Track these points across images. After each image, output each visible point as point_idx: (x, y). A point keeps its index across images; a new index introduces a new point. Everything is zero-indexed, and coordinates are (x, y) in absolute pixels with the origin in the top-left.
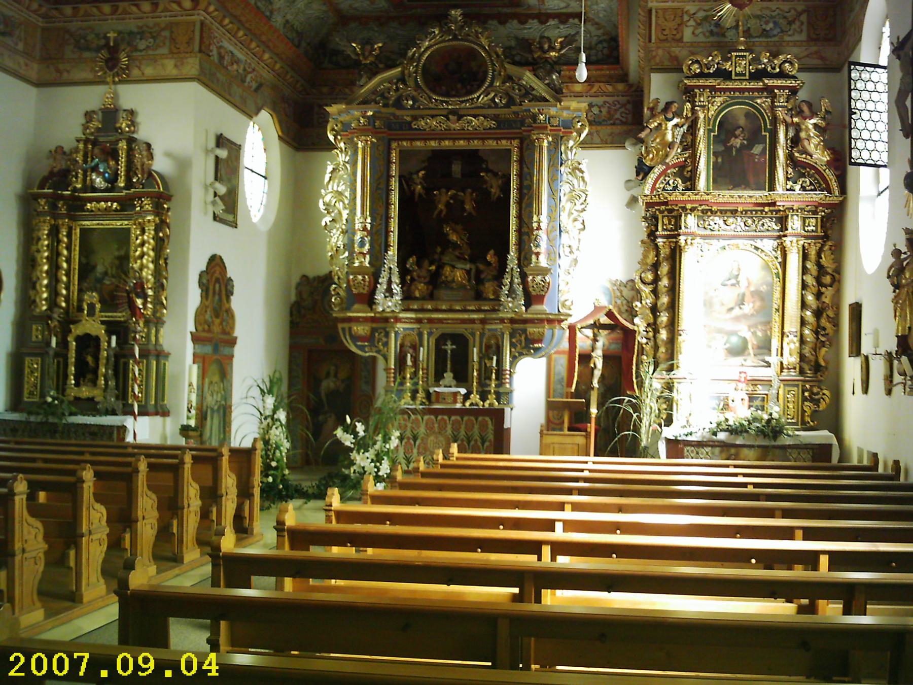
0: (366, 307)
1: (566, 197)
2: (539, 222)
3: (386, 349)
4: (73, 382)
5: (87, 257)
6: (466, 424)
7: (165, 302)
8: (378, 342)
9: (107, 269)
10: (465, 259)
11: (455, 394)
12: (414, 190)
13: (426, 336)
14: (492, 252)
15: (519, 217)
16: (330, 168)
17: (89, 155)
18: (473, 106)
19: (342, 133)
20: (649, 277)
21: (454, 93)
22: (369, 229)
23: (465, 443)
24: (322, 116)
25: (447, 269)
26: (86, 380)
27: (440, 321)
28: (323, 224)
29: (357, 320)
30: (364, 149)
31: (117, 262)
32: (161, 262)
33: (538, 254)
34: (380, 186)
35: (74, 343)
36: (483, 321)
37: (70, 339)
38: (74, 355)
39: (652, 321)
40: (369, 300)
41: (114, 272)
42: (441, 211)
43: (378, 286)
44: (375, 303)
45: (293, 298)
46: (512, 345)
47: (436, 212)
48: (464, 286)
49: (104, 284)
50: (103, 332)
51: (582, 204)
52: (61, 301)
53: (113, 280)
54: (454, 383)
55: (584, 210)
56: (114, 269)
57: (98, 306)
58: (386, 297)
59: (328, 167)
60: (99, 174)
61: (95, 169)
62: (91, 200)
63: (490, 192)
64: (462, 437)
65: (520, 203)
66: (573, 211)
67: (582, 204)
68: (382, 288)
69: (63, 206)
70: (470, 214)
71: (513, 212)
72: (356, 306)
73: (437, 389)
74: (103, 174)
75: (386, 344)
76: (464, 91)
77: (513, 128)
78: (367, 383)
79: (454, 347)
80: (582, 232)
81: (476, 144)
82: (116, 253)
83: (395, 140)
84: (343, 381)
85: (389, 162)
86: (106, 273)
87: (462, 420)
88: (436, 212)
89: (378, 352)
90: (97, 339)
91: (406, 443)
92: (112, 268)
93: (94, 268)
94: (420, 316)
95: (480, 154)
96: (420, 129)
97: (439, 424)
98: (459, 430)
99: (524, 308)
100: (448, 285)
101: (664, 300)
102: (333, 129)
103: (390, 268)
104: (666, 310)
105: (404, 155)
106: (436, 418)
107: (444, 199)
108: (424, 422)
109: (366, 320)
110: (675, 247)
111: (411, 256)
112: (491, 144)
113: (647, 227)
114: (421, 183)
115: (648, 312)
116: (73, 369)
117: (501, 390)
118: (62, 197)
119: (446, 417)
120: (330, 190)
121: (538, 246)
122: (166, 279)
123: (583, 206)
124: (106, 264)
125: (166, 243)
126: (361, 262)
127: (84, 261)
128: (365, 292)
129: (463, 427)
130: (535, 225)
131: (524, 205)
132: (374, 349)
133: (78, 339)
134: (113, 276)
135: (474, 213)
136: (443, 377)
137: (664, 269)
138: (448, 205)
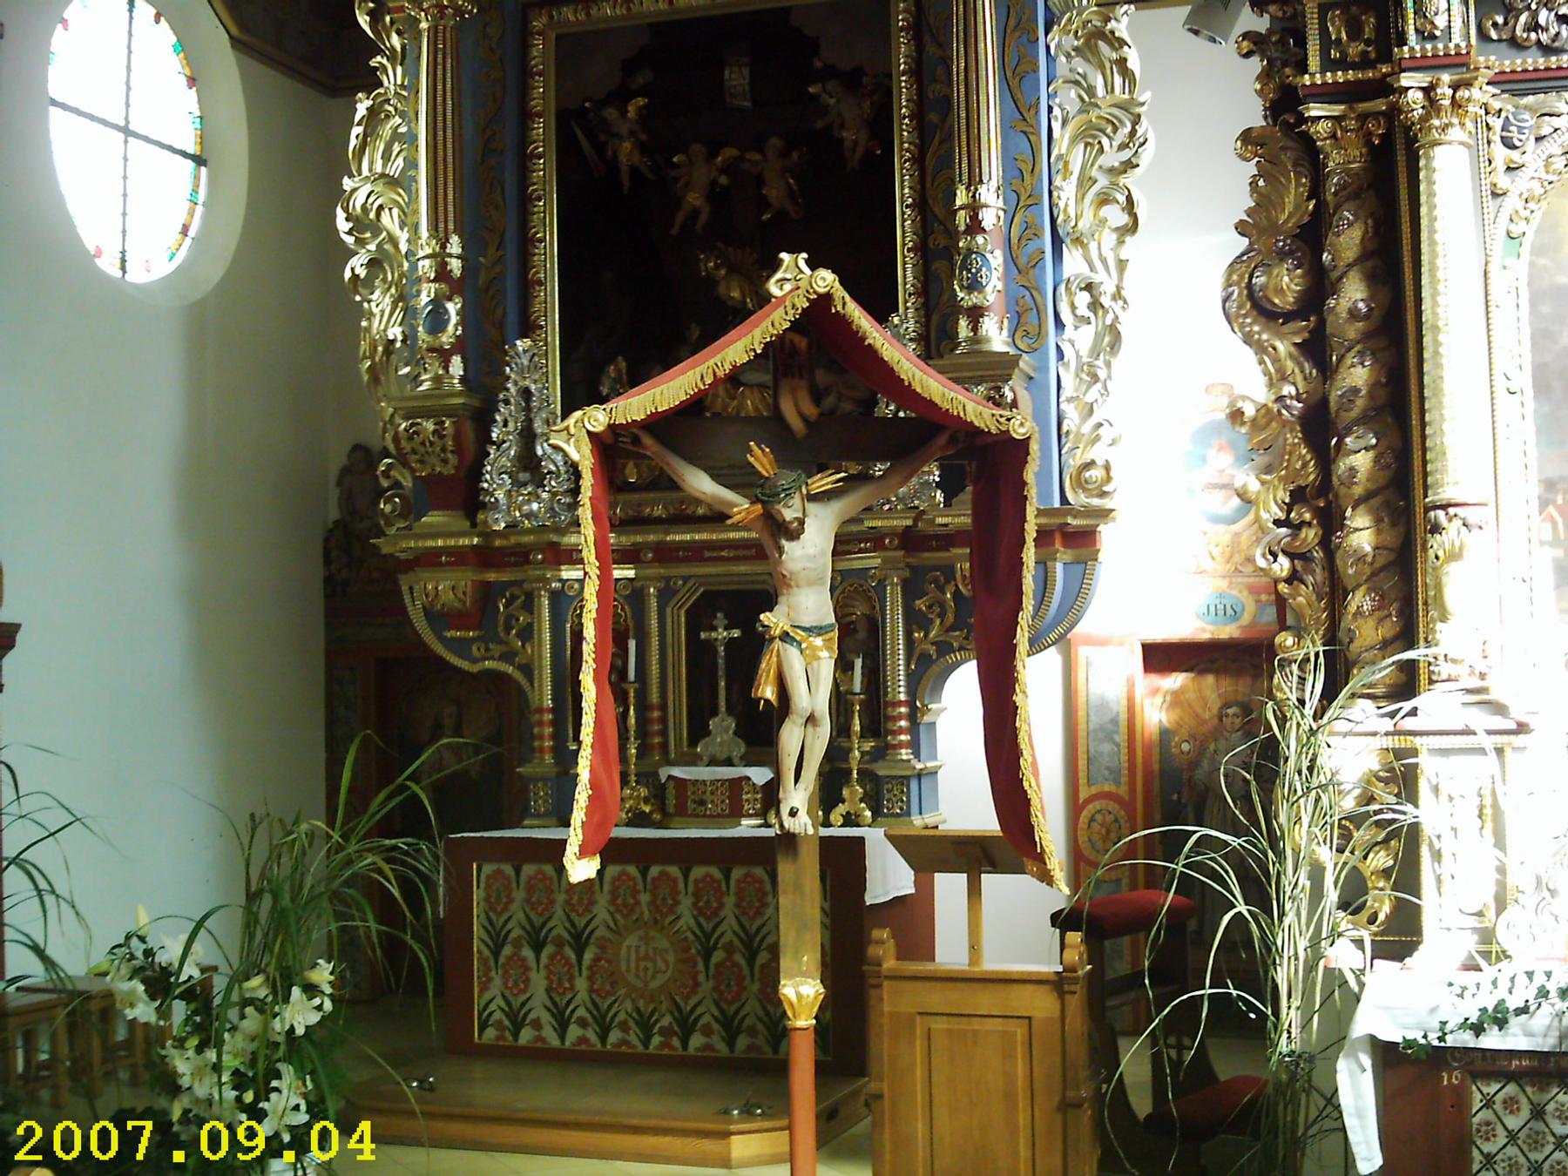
1: (1071, 127)
2: (974, 208)
6: (740, 891)
8: (508, 629)
11: (737, 785)
12: (615, 157)
15: (921, 205)
16: (362, 109)
20: (1287, 283)
22: (457, 272)
23: (739, 958)
28: (348, 274)
29: (429, 559)
33: (976, 314)
39: (1311, 475)
40: (471, 501)
42: (696, 212)
44: (484, 506)
45: (334, 513)
46: (914, 620)
47: (680, 218)
51: (1123, 146)
54: (740, 749)
55: (1130, 165)
63: (841, 141)
64: (728, 936)
65: (919, 160)
66: (1094, 173)
67: (1123, 146)
71: (903, 191)
72: (433, 519)
73: (677, 772)
75: (527, 633)
79: (736, 633)
80: (1128, 239)
87: (727, 878)
88: (680, 218)
89: (508, 657)
91: (552, 957)
97: (654, 895)
98: (716, 913)
99: (939, 496)
101: (1357, 375)
103: (526, 394)
104: (1363, 420)
105: (570, 48)
106: (644, 873)
107: (701, 175)
109: (459, 558)
110: (1387, 138)
111: (611, 359)
113: (1264, 76)
114: (632, 133)
115: (1294, 438)
117: (882, 770)
119: (674, 870)
120: (365, 172)
121: (974, 286)
123: (1127, 154)
126: (437, 380)
128: (449, 470)
129: (730, 900)
130: (962, 219)
131: (930, 163)
137: (1348, 240)
138: (715, 195)
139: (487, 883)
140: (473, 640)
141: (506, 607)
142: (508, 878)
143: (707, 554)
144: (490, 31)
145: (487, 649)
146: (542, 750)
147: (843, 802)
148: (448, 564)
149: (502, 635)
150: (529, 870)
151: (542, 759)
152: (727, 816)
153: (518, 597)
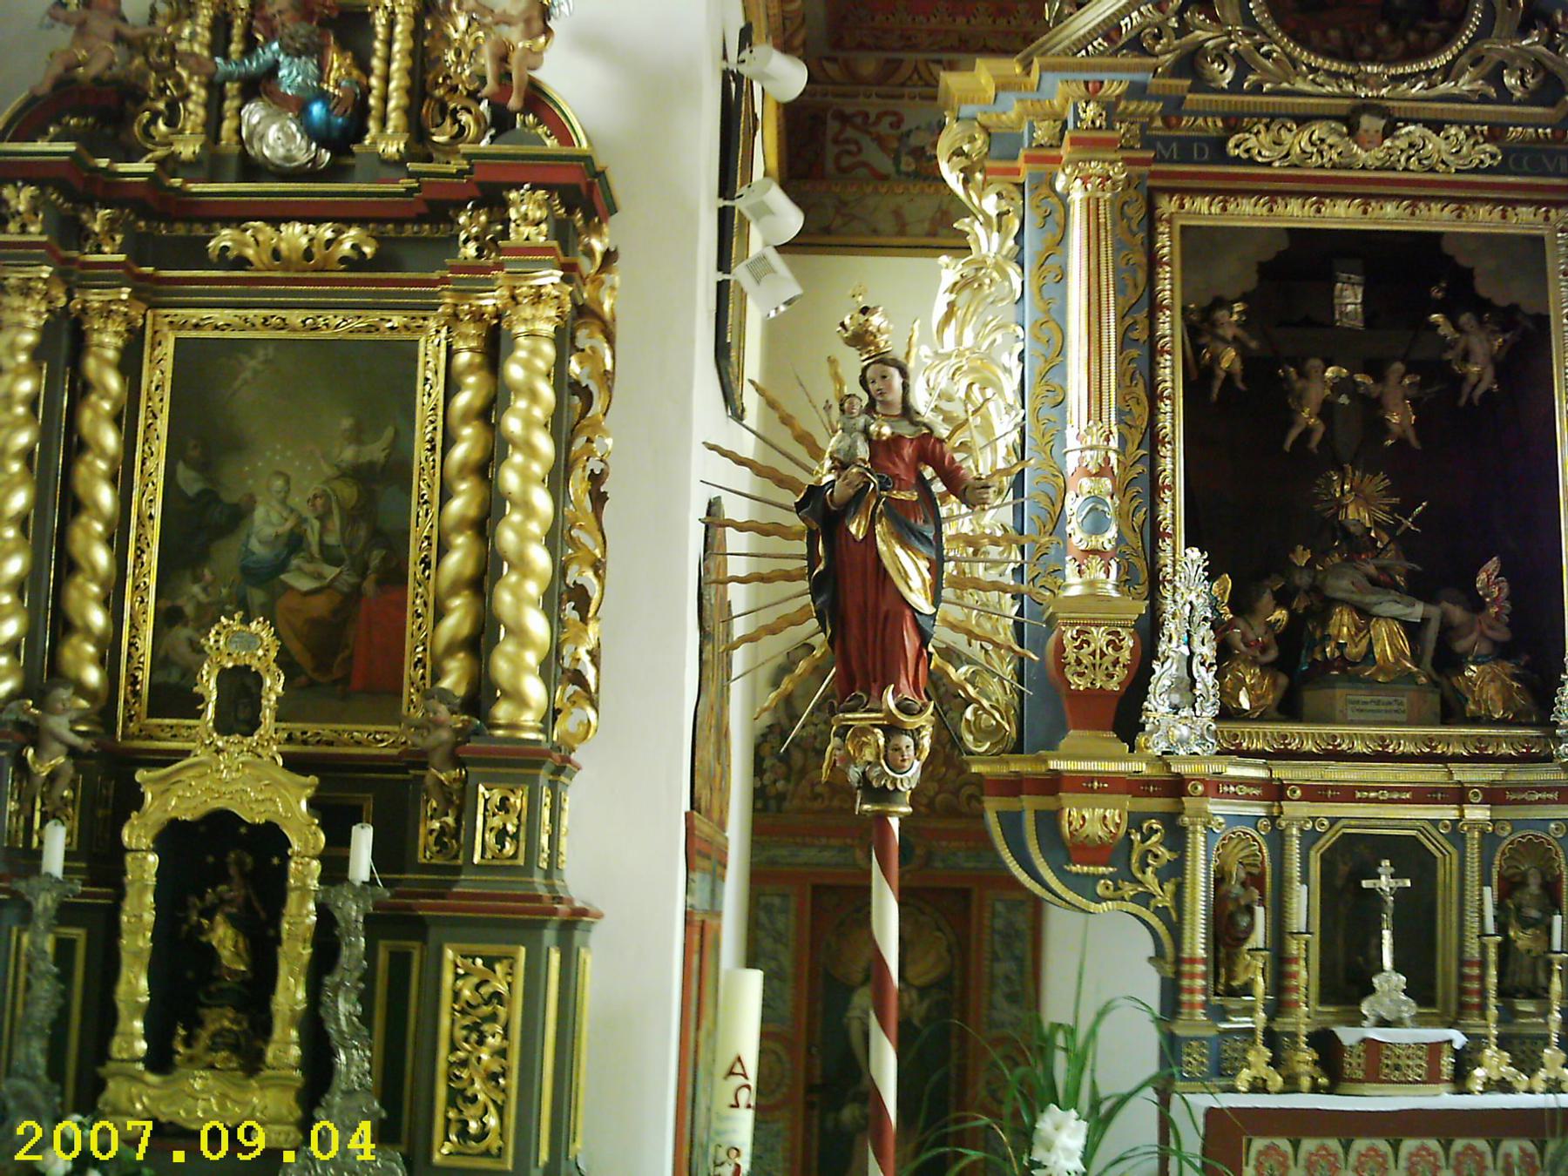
0: (1108, 740)
3: (1169, 887)
4: (142, 1046)
5: (205, 467)
7: (590, 674)
8: (1144, 865)
9: (302, 520)
10: (1396, 587)
11: (1434, 1049)
12: (1216, 359)
13: (1295, 844)
14: (1493, 565)
17: (237, 31)
18: (1432, 93)
19: (988, 164)
21: (1367, 49)
24: (853, 148)
25: (1343, 624)
26: (204, 1037)
27: (1347, 794)
29: (1082, 784)
30: (1092, 205)
31: (348, 492)
32: (578, 487)
34: (1135, 335)
35: (153, 859)
36: (1493, 796)
37: (137, 834)
38: (149, 917)
41: (332, 539)
42: (1307, 432)
43: (1156, 665)
47: (1293, 434)
48: (1411, 677)
49: (288, 588)
50: (303, 805)
52: (80, 660)
53: (331, 572)
54: (1409, 1008)
56: (336, 521)
57: (274, 686)
58: (1175, 709)
59: (944, 272)
60: (280, 103)
61: (258, 86)
62: (236, 216)
68: (1164, 674)
69: (110, 233)
70: (1402, 442)
74: (300, 108)
75: (1175, 871)
76: (1400, 46)
77: (1545, 174)
78: (1013, 998)
81: (1436, 218)
82: (349, 454)
83: (1171, 192)
84: (923, 991)
85: (1153, 262)
86: (295, 542)
88: (1293, 434)
90: (271, 838)
92: (323, 518)
93: (239, 515)
94: (1284, 772)
95: (1448, 248)
96: (1251, 162)
100: (1352, 669)
102: (959, 153)
106: (1446, 1147)
107: (1316, 393)
108: (1403, 1163)
112: (1483, 219)
116: (143, 983)
118: (108, 191)
122: (598, 567)
124: (296, 500)
125: (597, 407)
126: (1092, 584)
127: (191, 483)
128: (1113, 686)
132: (1129, 890)
133: (173, 837)
134: (329, 555)
135: (1411, 435)
136: (1371, 990)
138: (1327, 410)
139: (1257, 1160)
140: (1103, 876)
141: (1143, 841)
142: (1284, 1155)
143: (1358, 795)
144: (1128, 210)
145: (1117, 888)
146: (1192, 1005)
147: (1543, 1066)
148: (1101, 790)
149: (1139, 876)
150: (1309, 1145)
151: (1192, 1015)
152: (1424, 1082)
153: (1156, 831)
